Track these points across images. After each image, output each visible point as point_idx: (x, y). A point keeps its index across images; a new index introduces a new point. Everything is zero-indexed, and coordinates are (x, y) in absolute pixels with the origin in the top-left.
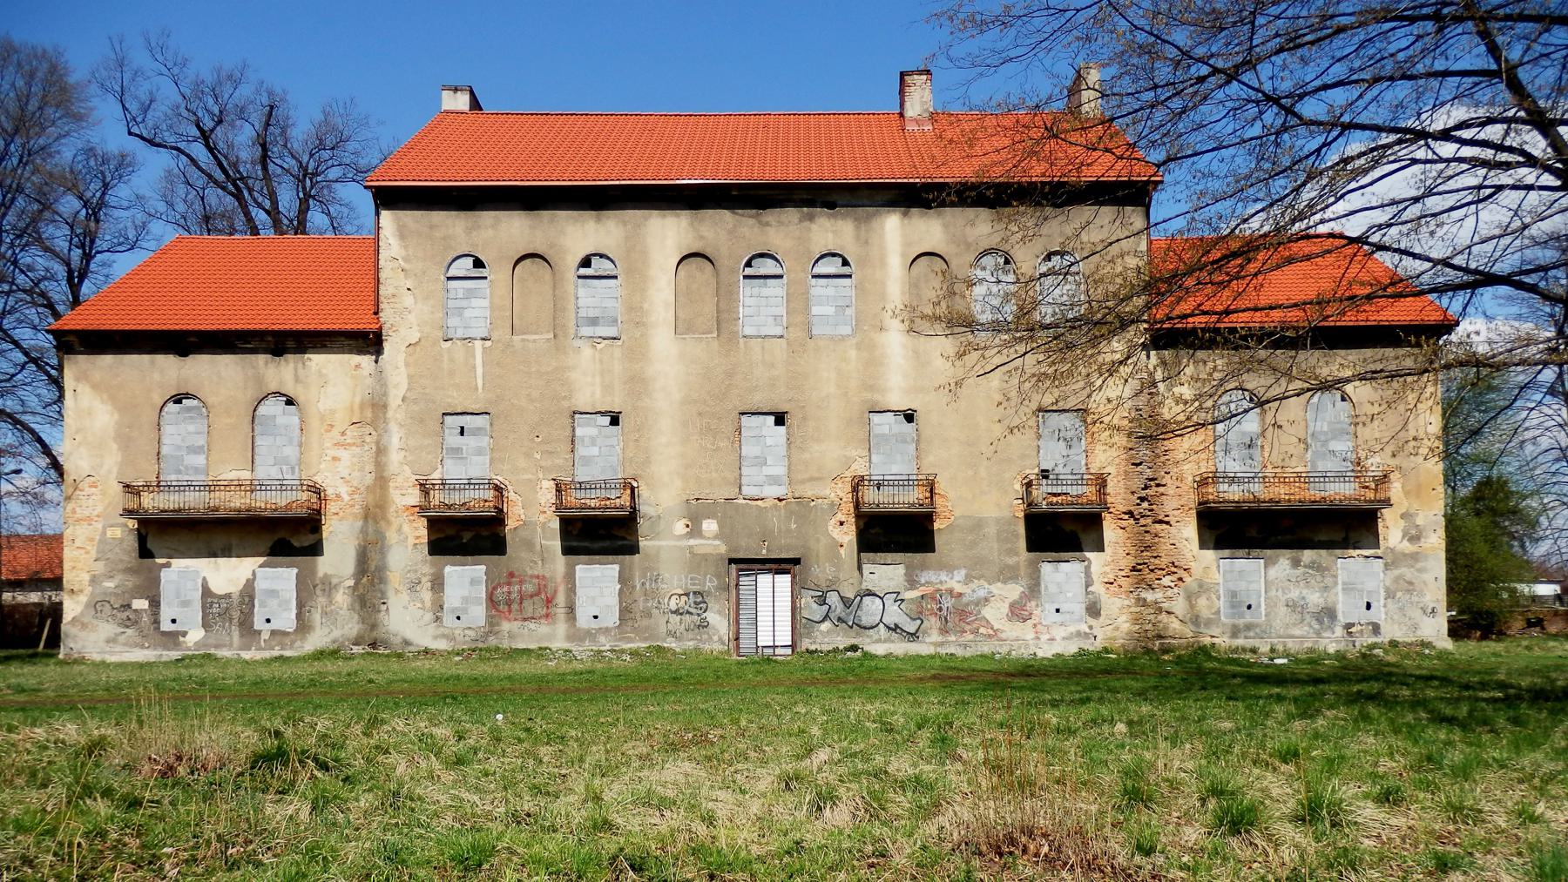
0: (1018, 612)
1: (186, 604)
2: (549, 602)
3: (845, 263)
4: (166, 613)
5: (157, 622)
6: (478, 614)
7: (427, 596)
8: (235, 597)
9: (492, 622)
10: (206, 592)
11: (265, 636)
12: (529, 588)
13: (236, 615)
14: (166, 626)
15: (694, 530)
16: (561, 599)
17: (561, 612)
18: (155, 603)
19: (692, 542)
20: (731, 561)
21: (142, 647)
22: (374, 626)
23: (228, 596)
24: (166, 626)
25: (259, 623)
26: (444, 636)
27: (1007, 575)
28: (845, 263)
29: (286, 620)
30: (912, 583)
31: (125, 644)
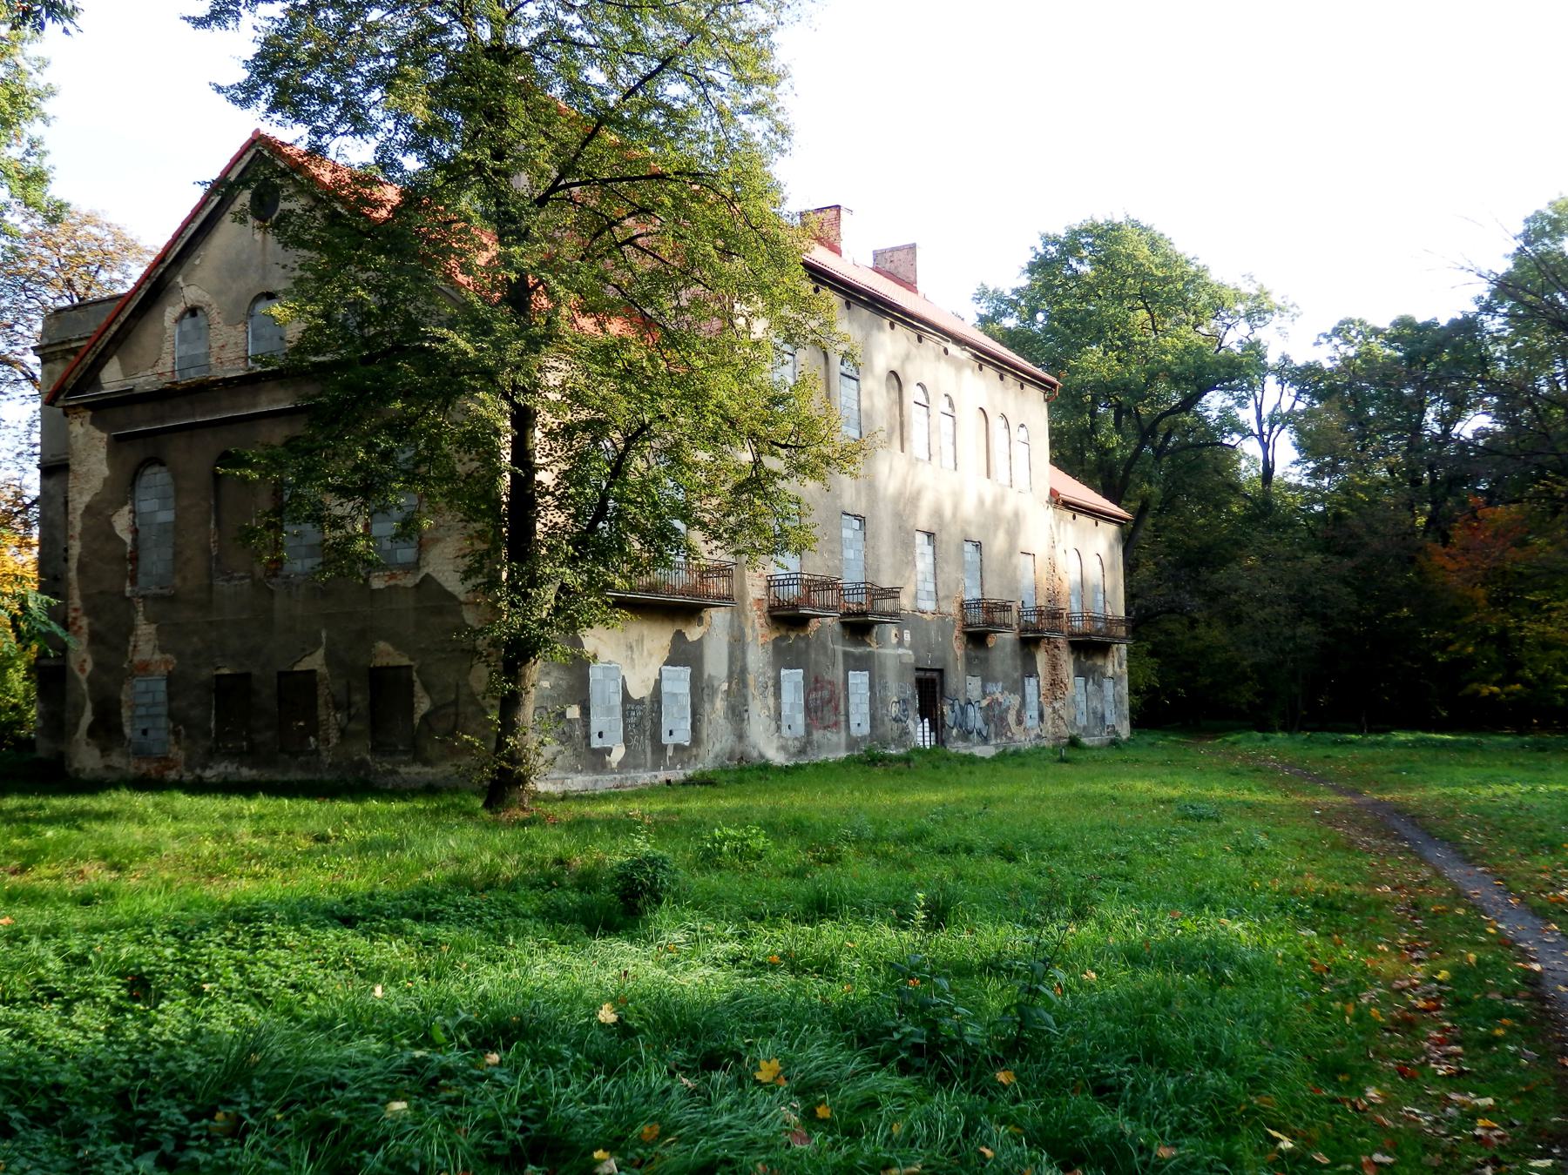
0: (1020, 722)
1: (609, 711)
2: (836, 708)
3: (951, 404)
4: (597, 723)
5: (587, 736)
6: (800, 719)
7: (771, 701)
8: (647, 701)
9: (808, 733)
10: (626, 697)
11: (670, 753)
12: (826, 694)
13: (648, 725)
14: (596, 743)
15: (900, 643)
16: (842, 707)
17: (842, 718)
18: (586, 711)
19: (901, 651)
20: (918, 669)
21: (577, 772)
22: (741, 736)
23: (641, 701)
24: (596, 743)
26: (783, 748)
27: (1013, 691)
28: (951, 404)
29: (683, 736)
30: (984, 694)
31: (561, 768)
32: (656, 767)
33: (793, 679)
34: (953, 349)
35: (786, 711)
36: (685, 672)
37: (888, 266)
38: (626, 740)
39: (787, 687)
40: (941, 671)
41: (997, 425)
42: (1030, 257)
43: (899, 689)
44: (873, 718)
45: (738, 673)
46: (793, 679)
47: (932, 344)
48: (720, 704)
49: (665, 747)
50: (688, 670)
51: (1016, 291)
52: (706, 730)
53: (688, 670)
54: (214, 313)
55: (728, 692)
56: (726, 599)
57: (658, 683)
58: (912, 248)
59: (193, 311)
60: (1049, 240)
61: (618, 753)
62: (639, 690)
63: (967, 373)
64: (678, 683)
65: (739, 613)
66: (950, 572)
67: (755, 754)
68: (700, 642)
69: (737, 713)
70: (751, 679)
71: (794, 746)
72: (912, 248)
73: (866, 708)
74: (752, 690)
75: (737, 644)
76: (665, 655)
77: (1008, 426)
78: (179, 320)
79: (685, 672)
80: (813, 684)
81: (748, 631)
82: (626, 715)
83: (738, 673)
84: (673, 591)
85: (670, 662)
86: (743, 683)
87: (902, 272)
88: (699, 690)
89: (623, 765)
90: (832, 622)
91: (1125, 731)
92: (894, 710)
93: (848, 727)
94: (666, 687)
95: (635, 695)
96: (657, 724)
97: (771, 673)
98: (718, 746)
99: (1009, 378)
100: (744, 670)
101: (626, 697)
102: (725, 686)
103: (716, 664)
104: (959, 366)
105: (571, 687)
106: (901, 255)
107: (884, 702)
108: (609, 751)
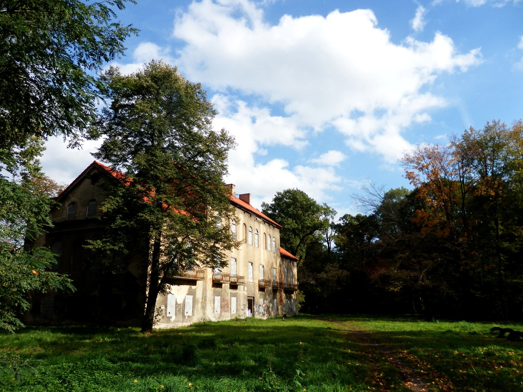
5: (166, 313)
7: (212, 304)
9: (221, 313)
10: (176, 303)
11: (186, 318)
12: (226, 303)
13: (181, 310)
14: (168, 315)
15: (244, 290)
18: (166, 307)
22: (204, 314)
23: (180, 304)
24: (168, 315)
25: (186, 314)
26: (215, 317)
29: (190, 314)
32: (183, 322)
33: (218, 299)
34: (258, 219)
35: (216, 307)
36: (191, 297)
37: (243, 198)
38: (176, 315)
39: (216, 301)
40: (254, 297)
41: (268, 237)
42: (274, 197)
43: (244, 302)
44: (237, 309)
45: (204, 298)
46: (218, 299)
47: (253, 217)
48: (200, 305)
49: (185, 317)
50: (192, 296)
51: (271, 205)
52: (195, 312)
53: (192, 296)
54: (78, 204)
55: (202, 302)
56: (203, 278)
57: (185, 300)
58: (248, 195)
59: (73, 203)
60: (279, 194)
61: (173, 318)
62: (180, 301)
63: (261, 225)
64: (189, 299)
65: (205, 282)
66: (256, 272)
67: (208, 318)
68: (195, 289)
69: (204, 308)
70: (207, 299)
71: (217, 316)
72: (248, 195)
73: (235, 307)
74: (208, 302)
75: (205, 290)
76: (187, 292)
77: (270, 237)
78: (69, 205)
79: (191, 297)
80: (223, 300)
81: (207, 287)
82: (176, 308)
83: (204, 298)
84: (189, 276)
85: (188, 294)
86: (205, 300)
87: (246, 200)
88: (194, 301)
89: (175, 321)
90: (228, 285)
91: (297, 313)
92: (242, 307)
93: (231, 311)
94: (186, 301)
95: (179, 302)
96: (184, 310)
97: (212, 297)
98: (199, 316)
99: (271, 226)
100: (206, 297)
101: (176, 303)
102: (201, 301)
103: (199, 295)
104: (259, 223)
105: (163, 301)
106: (245, 196)
107: (240, 305)
108: (171, 317)
